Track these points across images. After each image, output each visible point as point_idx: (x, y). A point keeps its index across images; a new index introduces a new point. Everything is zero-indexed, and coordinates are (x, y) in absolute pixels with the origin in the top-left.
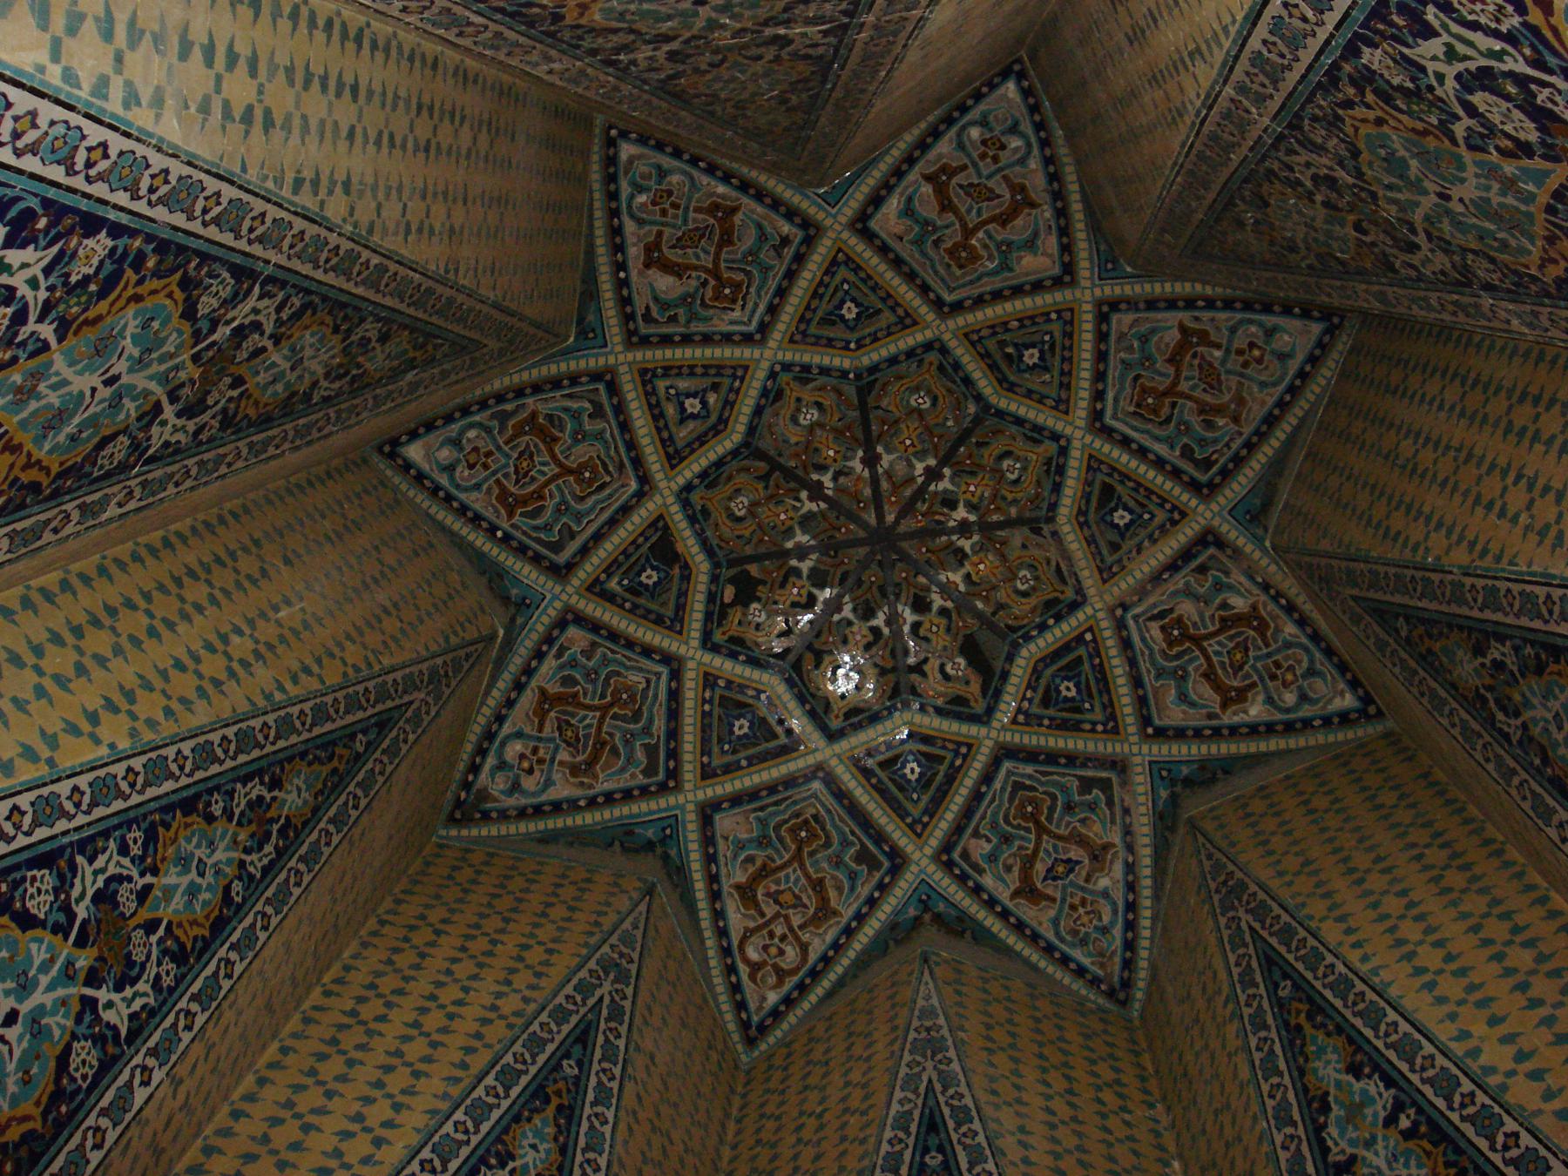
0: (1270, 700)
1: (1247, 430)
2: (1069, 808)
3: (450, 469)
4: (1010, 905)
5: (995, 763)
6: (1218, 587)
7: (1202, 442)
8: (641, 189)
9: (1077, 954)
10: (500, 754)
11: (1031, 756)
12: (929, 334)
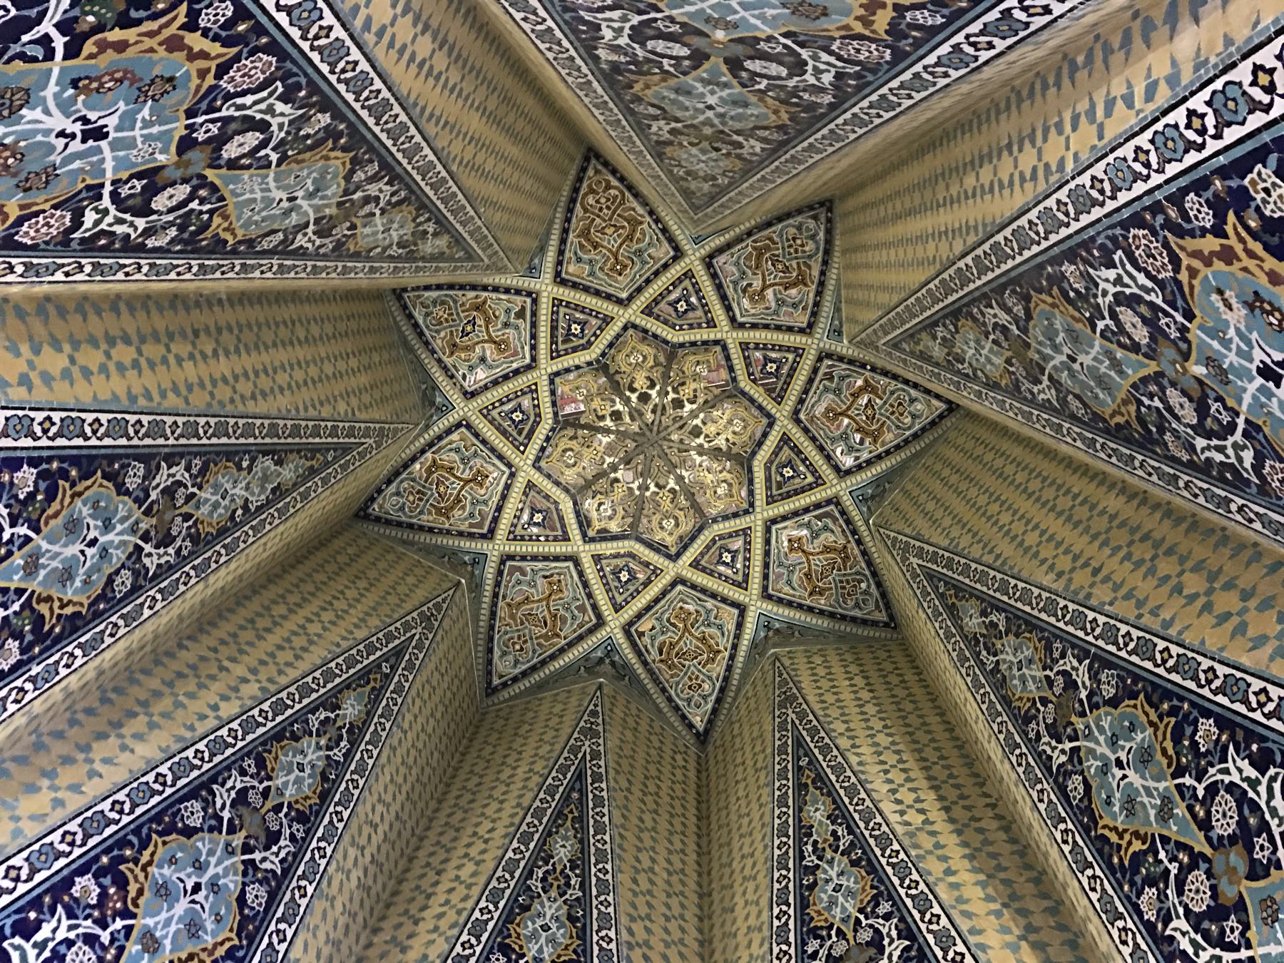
0: (413, 480)
1: (500, 604)
2: (483, 360)
3: (912, 401)
4: (485, 294)
5: (534, 359)
6: (472, 515)
7: (519, 582)
8: (866, 592)
9: (434, 294)
10: (817, 242)
11: (517, 372)
12: (680, 562)
